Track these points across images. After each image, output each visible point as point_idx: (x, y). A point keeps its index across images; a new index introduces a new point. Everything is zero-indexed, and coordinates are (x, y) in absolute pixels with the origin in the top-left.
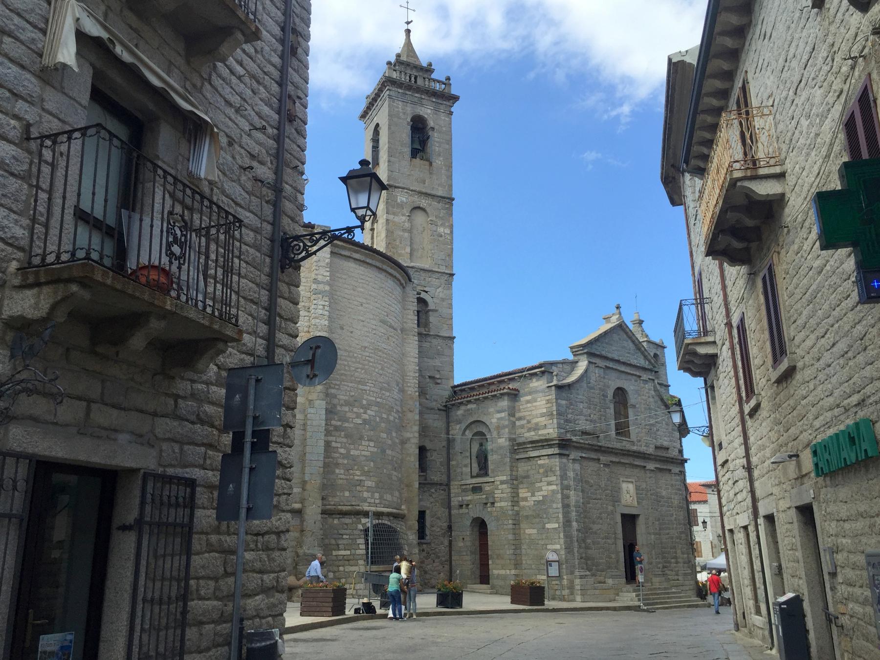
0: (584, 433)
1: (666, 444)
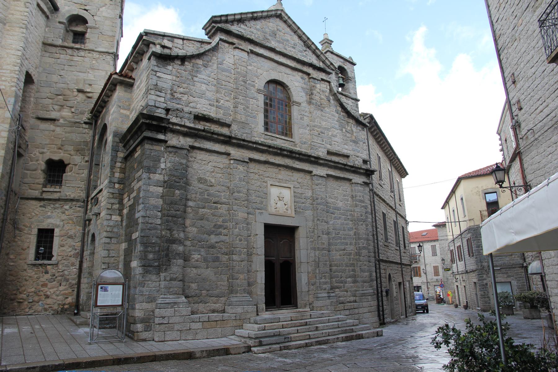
0: (199, 118)
1: (345, 152)
